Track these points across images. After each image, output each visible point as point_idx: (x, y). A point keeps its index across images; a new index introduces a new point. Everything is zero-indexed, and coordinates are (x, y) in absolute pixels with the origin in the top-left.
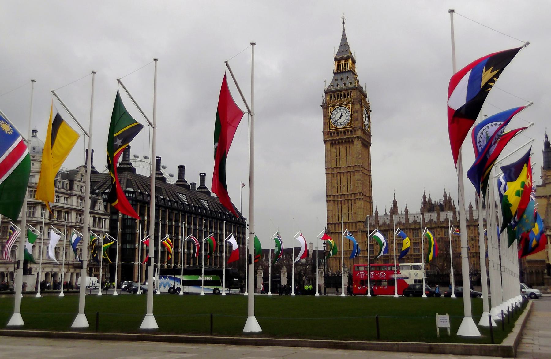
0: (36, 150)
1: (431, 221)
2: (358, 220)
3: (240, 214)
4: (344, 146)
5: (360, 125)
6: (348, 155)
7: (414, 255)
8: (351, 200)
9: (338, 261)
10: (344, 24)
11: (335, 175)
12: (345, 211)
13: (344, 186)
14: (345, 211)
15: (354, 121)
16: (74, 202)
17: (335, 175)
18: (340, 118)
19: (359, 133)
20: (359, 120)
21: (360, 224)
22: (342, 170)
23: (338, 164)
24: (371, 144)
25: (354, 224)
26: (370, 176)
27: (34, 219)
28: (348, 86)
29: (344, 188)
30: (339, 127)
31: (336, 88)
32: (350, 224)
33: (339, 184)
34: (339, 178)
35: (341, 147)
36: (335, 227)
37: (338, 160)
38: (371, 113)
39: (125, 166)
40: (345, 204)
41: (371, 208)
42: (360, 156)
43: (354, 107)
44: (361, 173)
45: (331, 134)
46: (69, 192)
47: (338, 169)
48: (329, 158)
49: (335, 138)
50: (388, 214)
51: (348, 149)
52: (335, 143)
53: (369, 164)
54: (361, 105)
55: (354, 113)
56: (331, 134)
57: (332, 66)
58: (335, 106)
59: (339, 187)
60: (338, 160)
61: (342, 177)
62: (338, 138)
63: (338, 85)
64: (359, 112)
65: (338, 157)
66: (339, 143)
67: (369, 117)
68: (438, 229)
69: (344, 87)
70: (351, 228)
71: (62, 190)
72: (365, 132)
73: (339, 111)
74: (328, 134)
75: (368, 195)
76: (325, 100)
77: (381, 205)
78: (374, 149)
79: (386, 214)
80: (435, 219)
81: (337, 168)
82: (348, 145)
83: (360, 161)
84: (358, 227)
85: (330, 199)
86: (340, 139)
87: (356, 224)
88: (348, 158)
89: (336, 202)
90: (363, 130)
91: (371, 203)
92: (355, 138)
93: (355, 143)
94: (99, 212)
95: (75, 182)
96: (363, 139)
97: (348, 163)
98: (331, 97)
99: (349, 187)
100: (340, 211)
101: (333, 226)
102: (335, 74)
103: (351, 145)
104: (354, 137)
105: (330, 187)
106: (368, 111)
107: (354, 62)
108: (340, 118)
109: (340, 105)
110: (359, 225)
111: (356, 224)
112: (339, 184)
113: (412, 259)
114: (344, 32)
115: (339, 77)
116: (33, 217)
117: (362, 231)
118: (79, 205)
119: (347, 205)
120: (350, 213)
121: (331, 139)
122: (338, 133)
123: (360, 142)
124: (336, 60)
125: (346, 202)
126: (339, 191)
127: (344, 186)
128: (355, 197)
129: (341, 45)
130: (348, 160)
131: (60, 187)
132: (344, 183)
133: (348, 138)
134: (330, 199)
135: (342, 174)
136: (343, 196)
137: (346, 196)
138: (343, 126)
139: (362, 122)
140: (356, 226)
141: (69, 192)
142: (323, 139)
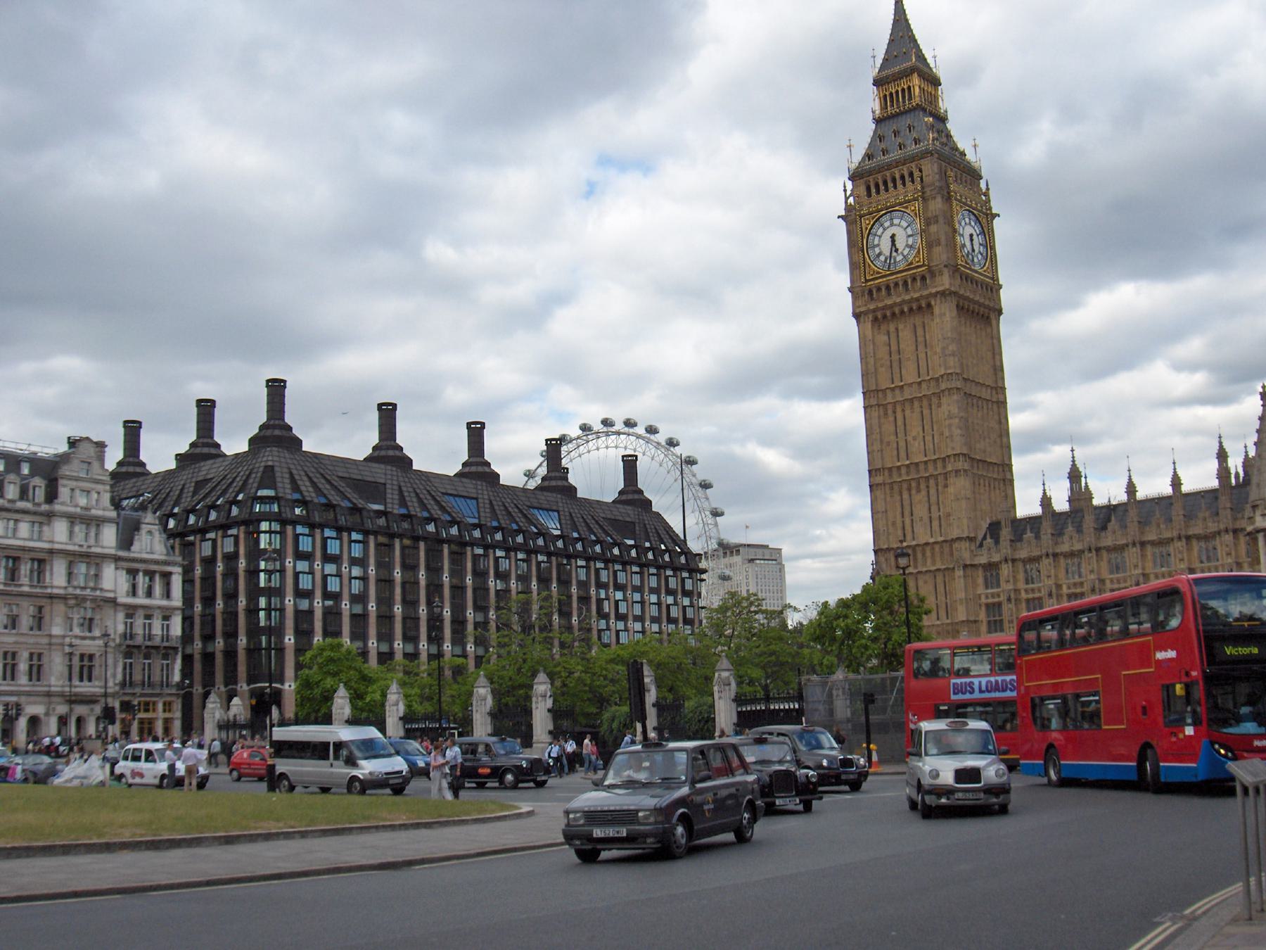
2: (955, 533)
8: (936, 477)
11: (890, 408)
12: (921, 511)
13: (914, 439)
14: (921, 511)
16: (59, 533)
17: (890, 408)
19: (945, 282)
22: (907, 394)
24: (1000, 312)
25: (946, 548)
28: (912, 148)
31: (880, 159)
35: (901, 327)
37: (895, 365)
40: (919, 491)
42: (952, 347)
46: (45, 507)
48: (872, 361)
49: (882, 300)
51: (920, 331)
52: (885, 317)
53: (998, 370)
54: (948, 199)
55: (928, 222)
56: (870, 292)
57: (868, 102)
59: (902, 444)
60: (895, 365)
61: (908, 412)
62: (889, 302)
64: (941, 220)
66: (894, 314)
70: (938, 559)
71: (21, 505)
76: (851, 200)
77: (1035, 487)
81: (893, 389)
82: (918, 320)
86: (895, 304)
90: (955, 269)
93: (937, 310)
94: (145, 556)
95: (61, 482)
97: (923, 370)
98: (868, 189)
99: (928, 438)
100: (907, 513)
102: (878, 121)
105: (877, 446)
109: (889, 210)
115: (888, 129)
117: (965, 566)
119: (924, 493)
120: (935, 515)
121: (872, 307)
124: (878, 83)
125: (923, 486)
126: (903, 454)
127: (914, 439)
128: (944, 467)
129: (891, 41)
130: (923, 364)
131: (17, 496)
132: (915, 430)
133: (917, 300)
134: (879, 479)
135: (907, 405)
136: (912, 468)
137: (922, 467)
138: (901, 266)
139: (952, 245)
141: (45, 507)
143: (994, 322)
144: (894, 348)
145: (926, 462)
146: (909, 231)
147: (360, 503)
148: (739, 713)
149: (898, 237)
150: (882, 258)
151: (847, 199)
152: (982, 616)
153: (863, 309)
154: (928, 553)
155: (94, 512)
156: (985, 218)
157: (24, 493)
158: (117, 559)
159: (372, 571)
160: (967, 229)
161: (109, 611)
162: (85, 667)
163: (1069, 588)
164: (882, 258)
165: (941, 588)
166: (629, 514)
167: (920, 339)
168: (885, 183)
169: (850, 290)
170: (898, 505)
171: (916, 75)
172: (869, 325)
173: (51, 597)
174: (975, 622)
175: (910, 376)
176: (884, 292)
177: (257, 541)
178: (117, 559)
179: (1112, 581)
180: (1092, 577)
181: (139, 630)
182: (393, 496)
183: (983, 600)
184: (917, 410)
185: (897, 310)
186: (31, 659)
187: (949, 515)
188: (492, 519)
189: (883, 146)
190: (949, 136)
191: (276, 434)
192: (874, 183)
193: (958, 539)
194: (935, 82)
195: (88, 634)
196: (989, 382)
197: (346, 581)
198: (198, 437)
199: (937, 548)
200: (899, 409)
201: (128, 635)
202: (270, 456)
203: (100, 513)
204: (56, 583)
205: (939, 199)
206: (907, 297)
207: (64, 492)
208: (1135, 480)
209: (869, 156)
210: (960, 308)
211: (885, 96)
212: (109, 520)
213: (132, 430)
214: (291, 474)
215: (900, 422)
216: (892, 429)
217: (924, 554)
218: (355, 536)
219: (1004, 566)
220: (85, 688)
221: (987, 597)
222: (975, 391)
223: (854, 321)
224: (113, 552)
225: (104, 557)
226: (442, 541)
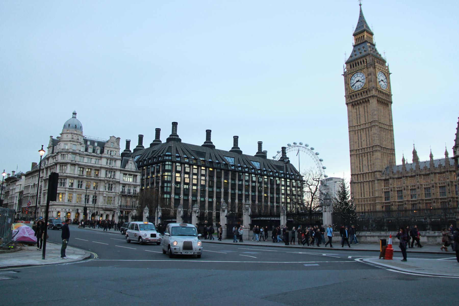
0: (78, 127)
2: (375, 170)
3: (298, 173)
4: (363, 105)
6: (366, 113)
7: (426, 200)
9: (360, 207)
10: (360, 5)
11: (356, 131)
12: (365, 163)
13: (364, 141)
14: (365, 163)
15: (369, 82)
16: (103, 162)
17: (356, 131)
22: (362, 127)
23: (359, 122)
24: (391, 103)
25: (373, 173)
26: (392, 130)
27: (65, 174)
28: (364, 53)
29: (364, 143)
30: (357, 89)
31: (354, 57)
32: (370, 174)
33: (360, 140)
34: (359, 134)
35: (360, 107)
36: (358, 177)
38: (391, 75)
39: (174, 137)
40: (365, 157)
44: (376, 128)
45: (351, 97)
47: (359, 127)
49: (355, 99)
51: (366, 108)
52: (355, 104)
53: (391, 120)
55: (368, 75)
56: (351, 97)
57: (352, 41)
59: (360, 142)
61: (362, 133)
62: (356, 99)
64: (372, 74)
65: (358, 116)
66: (358, 103)
68: (447, 173)
70: (370, 177)
76: (346, 70)
81: (357, 126)
82: (365, 105)
86: (358, 100)
88: (366, 115)
89: (358, 156)
90: (377, 89)
91: (394, 154)
92: (370, 97)
93: (370, 102)
94: (129, 170)
95: (105, 148)
97: (367, 120)
99: (368, 141)
100: (361, 163)
101: (356, 176)
102: (354, 46)
103: (368, 104)
109: (357, 72)
112: (360, 140)
114: (361, 11)
116: (65, 173)
117: (378, 180)
118: (108, 164)
119: (366, 157)
120: (369, 164)
121: (351, 101)
125: (366, 155)
129: (359, 22)
132: (364, 138)
133: (365, 99)
134: (352, 153)
135: (362, 131)
136: (363, 150)
137: (366, 149)
138: (360, 89)
141: (101, 155)
142: (345, 102)
143: (389, 106)
144: (358, 113)
145: (367, 148)
146: (363, 78)
147: (197, 157)
148: (252, 220)
149: (359, 80)
152: (383, 195)
153: (349, 102)
154: (367, 176)
155: (114, 157)
156: (387, 74)
157: (94, 151)
158: (121, 170)
159: (207, 178)
160: (381, 77)
161: (117, 185)
162: (109, 199)
165: (371, 187)
166: (282, 164)
167: (366, 111)
168: (356, 64)
169: (345, 96)
170: (358, 161)
172: (350, 107)
173: (100, 180)
174: (381, 197)
175: (362, 122)
176: (355, 97)
177: (165, 167)
178: (121, 170)
179: (424, 185)
180: (418, 184)
181: (126, 190)
182: (207, 155)
183: (384, 190)
184: (365, 132)
185: (359, 102)
186: (86, 197)
187: (373, 164)
188: (210, 159)
189: (355, 53)
190: (376, 50)
191: (174, 138)
192: (353, 64)
194: (372, 34)
195: (110, 191)
196: (388, 124)
197: (191, 180)
198: (156, 139)
199: (370, 174)
200: (359, 132)
201: (123, 192)
202: (172, 144)
203: (116, 157)
204: (102, 176)
205: (372, 68)
207: (106, 151)
208: (432, 153)
209: (351, 56)
210: (378, 101)
212: (119, 159)
213: (141, 138)
214: (176, 149)
215: (359, 136)
216: (357, 138)
217: (366, 176)
218: (203, 168)
219: (390, 180)
220: (109, 206)
222: (383, 126)
223: (346, 105)
224: (120, 168)
225: (117, 170)
226: (229, 170)
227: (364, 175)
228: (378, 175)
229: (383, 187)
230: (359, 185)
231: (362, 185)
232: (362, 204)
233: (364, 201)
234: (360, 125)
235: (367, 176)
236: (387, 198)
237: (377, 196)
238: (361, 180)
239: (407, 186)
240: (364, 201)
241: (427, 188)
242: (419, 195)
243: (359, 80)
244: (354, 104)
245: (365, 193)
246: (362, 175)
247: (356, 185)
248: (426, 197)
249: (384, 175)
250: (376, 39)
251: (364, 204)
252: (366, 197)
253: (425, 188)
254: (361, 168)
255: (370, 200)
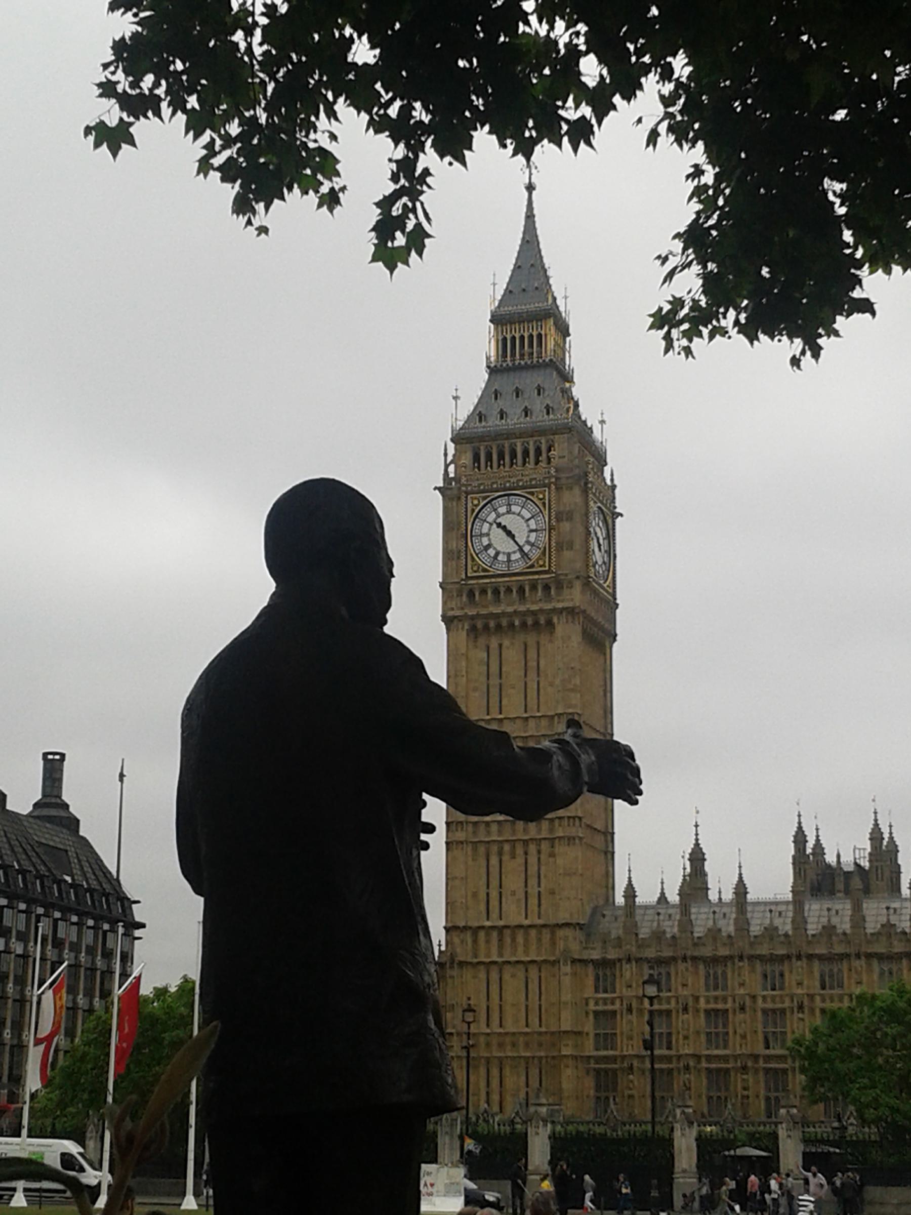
1: (829, 930)
4: (521, 637)
5: (579, 565)
6: (532, 675)
10: (530, 188)
12: (513, 882)
14: (513, 882)
15: (560, 547)
18: (510, 534)
20: (577, 546)
21: (568, 932)
24: (614, 637)
25: (546, 935)
28: (539, 418)
30: (502, 568)
31: (493, 423)
32: (533, 933)
35: (506, 643)
36: (475, 941)
37: (494, 692)
38: (619, 520)
40: (513, 856)
41: (609, 875)
43: (559, 500)
45: (471, 594)
50: (673, 897)
51: (532, 654)
52: (486, 627)
54: (585, 491)
56: (471, 594)
57: (482, 343)
58: (491, 494)
60: (494, 692)
63: (502, 415)
64: (577, 517)
65: (495, 681)
66: (499, 627)
67: (611, 536)
68: (856, 963)
69: (525, 423)
72: (595, 593)
73: (502, 510)
74: (460, 595)
75: (599, 825)
76: (452, 468)
78: (623, 655)
79: (663, 898)
80: (844, 924)
82: (531, 639)
83: (575, 699)
84: (561, 945)
85: (460, 835)
86: (504, 614)
87: (553, 934)
88: (532, 686)
89: (482, 849)
91: (609, 854)
92: (561, 611)
93: (559, 630)
96: (588, 618)
97: (533, 703)
98: (476, 458)
100: (495, 883)
102: (493, 371)
103: (544, 639)
104: (554, 610)
106: (610, 516)
107: (564, 330)
108: (510, 534)
109: (508, 492)
110: (566, 938)
111: (553, 934)
113: (756, 1071)
114: (530, 216)
115: (507, 384)
117: (574, 961)
119: (520, 860)
120: (533, 890)
121: (471, 612)
122: (496, 592)
123: (578, 628)
124: (497, 319)
125: (520, 850)
128: (551, 830)
129: (517, 267)
130: (533, 694)
133: (534, 613)
134: (460, 835)
138: (518, 567)
140: (553, 943)
144: (494, 668)
146: (533, 524)
150: (492, 552)
151: (447, 466)
152: (589, 1026)
153: (458, 613)
154: (520, 939)
163: (708, 1002)
164: (492, 552)
165: (534, 986)
167: (532, 664)
169: (441, 585)
171: (551, 321)
174: (579, 1033)
179: (764, 998)
180: (742, 991)
183: (592, 1006)
185: (504, 622)
187: (552, 893)
193: (567, 925)
205: (577, 491)
206: (522, 608)
209: (479, 415)
211: (505, 339)
217: (514, 940)
221: (596, 1004)
227: (507, 932)
228: (571, 941)
229: (589, 992)
230: (482, 975)
231: (494, 975)
232: (488, 1060)
233: (488, 1045)
234: (501, 720)
235: (508, 940)
236: (606, 1040)
237: (566, 1026)
238: (488, 955)
239: (697, 999)
240: (488, 1045)
241: (774, 1011)
242: (744, 1037)
243: (513, 532)
244: (479, 625)
245: (508, 1009)
246: (495, 934)
247: (468, 973)
248: (768, 1048)
249: (598, 945)
250: (580, 355)
251: (500, 1060)
252: (510, 1027)
253: (765, 1012)
254: (494, 903)
255: (527, 1045)
